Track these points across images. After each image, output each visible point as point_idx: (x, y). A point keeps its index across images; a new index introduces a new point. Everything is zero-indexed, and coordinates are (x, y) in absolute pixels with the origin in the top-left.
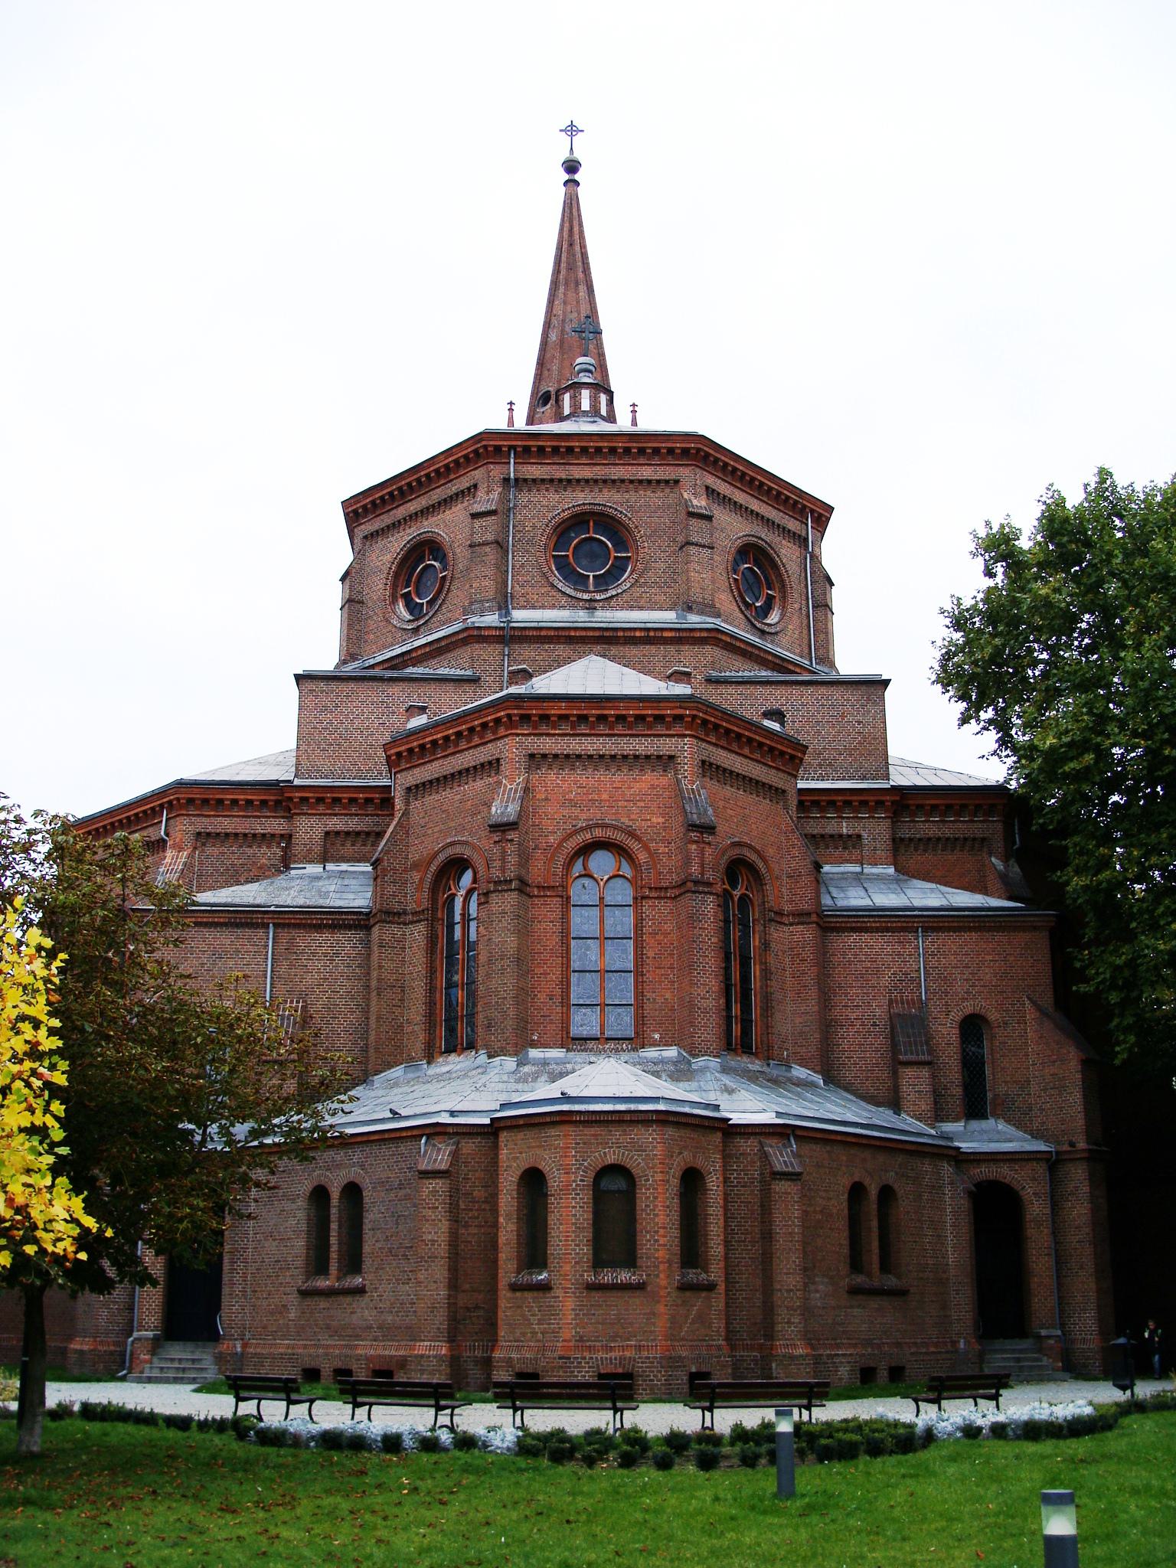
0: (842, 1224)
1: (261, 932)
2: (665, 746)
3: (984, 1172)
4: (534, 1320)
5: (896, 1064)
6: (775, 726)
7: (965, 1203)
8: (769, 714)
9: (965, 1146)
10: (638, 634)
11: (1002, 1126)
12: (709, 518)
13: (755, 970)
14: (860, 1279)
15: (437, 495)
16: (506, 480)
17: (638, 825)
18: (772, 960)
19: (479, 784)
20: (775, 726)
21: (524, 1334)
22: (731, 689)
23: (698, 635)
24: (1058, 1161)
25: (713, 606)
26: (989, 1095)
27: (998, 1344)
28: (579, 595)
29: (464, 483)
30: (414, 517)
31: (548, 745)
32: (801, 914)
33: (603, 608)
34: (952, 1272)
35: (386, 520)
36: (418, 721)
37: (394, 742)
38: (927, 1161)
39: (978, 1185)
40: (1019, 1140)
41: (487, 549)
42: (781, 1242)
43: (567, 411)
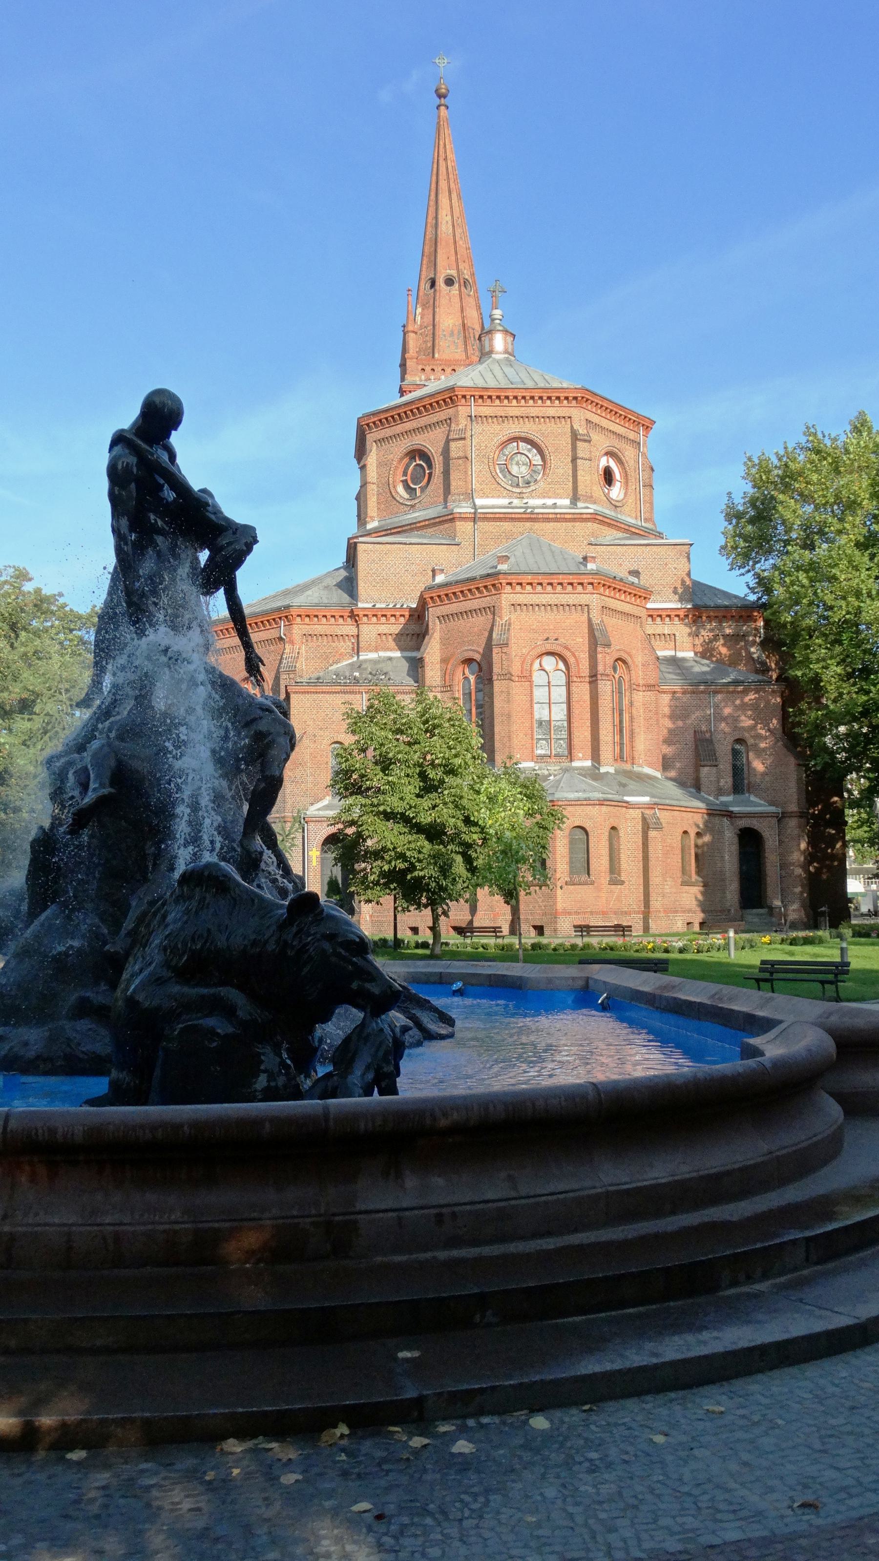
0: (678, 852)
1: (358, 696)
2: (584, 599)
3: (743, 823)
4: (540, 900)
5: (698, 767)
6: (636, 580)
7: (736, 840)
8: (630, 573)
9: (735, 809)
10: (551, 516)
11: (753, 798)
12: (590, 441)
13: (626, 717)
16: (471, 416)
17: (570, 643)
18: (634, 712)
20: (636, 580)
21: (534, 907)
23: (585, 516)
24: (783, 817)
25: (592, 497)
26: (746, 781)
27: (749, 911)
28: (514, 490)
31: (521, 599)
33: (528, 497)
34: (728, 874)
35: (388, 432)
36: (440, 579)
37: (430, 588)
38: (717, 818)
39: (740, 830)
41: (460, 461)
43: (487, 349)
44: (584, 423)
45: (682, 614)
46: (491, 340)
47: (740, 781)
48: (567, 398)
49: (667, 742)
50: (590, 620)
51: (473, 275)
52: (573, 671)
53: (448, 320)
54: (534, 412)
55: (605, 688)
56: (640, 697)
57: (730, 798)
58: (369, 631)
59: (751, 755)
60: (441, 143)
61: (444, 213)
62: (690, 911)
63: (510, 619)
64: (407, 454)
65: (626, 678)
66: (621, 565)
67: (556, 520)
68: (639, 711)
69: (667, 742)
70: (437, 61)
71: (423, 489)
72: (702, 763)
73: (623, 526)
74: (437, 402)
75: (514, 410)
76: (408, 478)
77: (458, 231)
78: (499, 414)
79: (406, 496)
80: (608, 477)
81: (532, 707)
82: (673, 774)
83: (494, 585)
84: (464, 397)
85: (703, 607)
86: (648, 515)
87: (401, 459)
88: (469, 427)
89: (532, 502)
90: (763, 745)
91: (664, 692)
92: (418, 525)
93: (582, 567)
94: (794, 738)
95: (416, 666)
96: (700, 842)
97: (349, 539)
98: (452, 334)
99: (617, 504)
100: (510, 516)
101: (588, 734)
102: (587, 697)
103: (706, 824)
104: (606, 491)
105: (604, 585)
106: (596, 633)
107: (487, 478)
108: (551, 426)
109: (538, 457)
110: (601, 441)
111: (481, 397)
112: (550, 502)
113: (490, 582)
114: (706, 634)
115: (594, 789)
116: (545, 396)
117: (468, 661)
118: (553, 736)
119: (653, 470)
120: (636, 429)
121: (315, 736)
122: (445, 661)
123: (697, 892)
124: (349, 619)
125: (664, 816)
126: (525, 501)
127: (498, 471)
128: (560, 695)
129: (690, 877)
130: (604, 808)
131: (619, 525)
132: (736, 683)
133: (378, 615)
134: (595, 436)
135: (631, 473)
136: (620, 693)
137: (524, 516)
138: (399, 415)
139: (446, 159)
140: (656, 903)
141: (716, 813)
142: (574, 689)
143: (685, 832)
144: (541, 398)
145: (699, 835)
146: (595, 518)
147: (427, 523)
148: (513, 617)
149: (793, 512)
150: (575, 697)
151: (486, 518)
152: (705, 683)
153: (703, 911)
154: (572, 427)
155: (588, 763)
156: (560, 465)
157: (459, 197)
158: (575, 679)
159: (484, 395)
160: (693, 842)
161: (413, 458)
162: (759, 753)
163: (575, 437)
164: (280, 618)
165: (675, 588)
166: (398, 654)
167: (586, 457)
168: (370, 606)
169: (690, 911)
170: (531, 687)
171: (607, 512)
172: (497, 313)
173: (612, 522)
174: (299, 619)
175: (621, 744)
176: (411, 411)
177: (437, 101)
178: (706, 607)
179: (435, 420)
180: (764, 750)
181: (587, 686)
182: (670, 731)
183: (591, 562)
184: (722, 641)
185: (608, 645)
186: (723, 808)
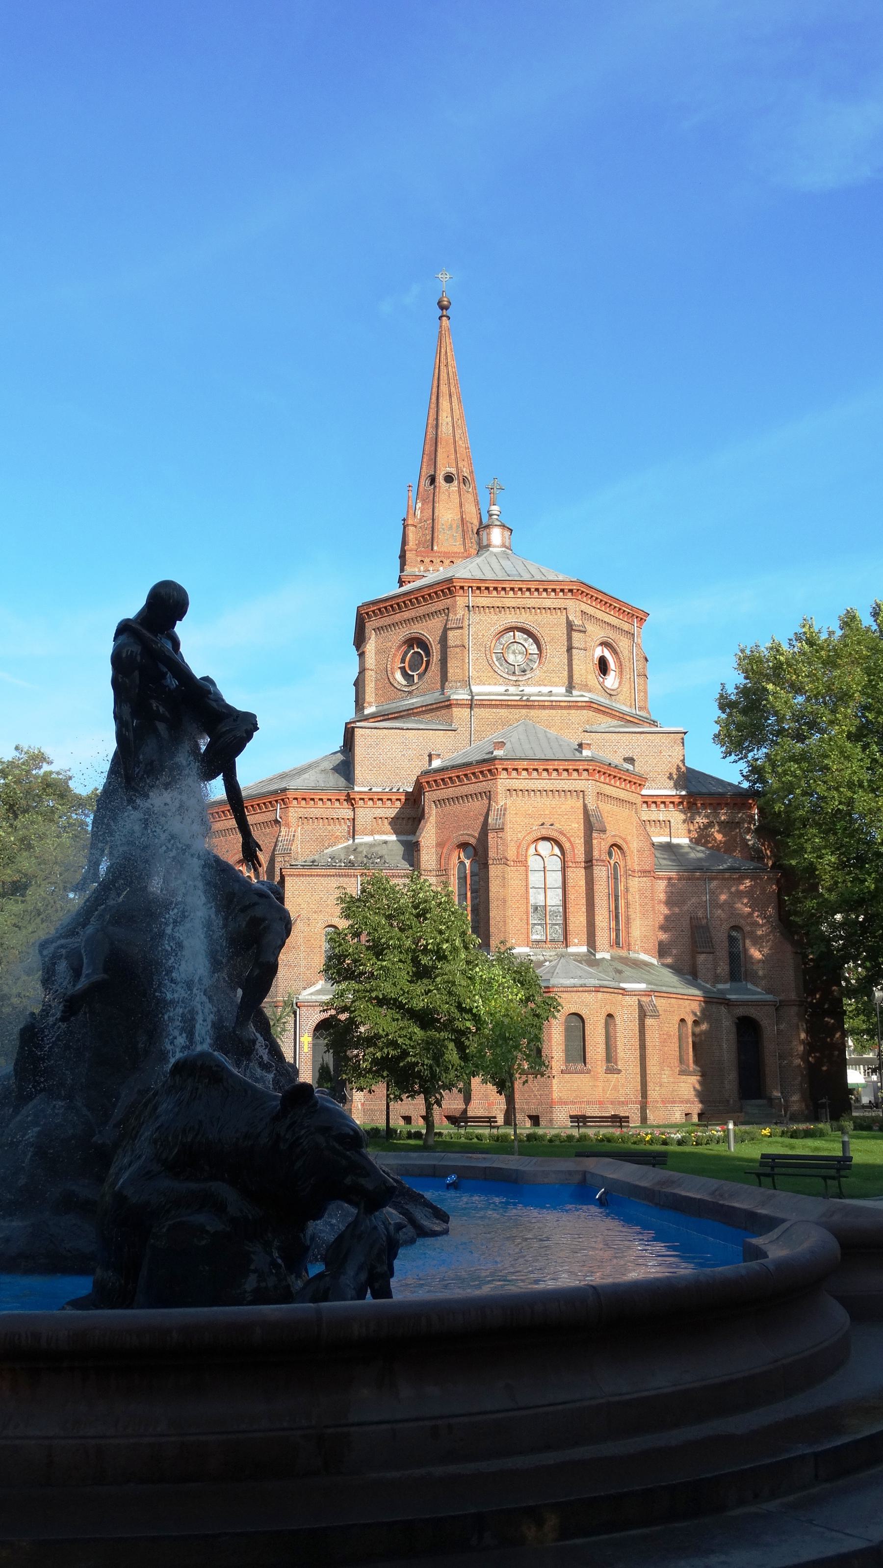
0: (676, 1040)
2: (580, 785)
3: (741, 1011)
6: (630, 767)
9: (733, 997)
10: (546, 704)
11: (750, 986)
13: (622, 903)
14: (684, 1067)
15: (422, 611)
16: (468, 607)
17: (566, 828)
19: (478, 805)
20: (630, 767)
21: (530, 1096)
22: (598, 735)
23: (580, 704)
25: (587, 685)
26: (743, 969)
28: (511, 677)
29: (440, 605)
30: (407, 621)
32: (645, 872)
33: (524, 685)
35: (386, 621)
36: (436, 763)
37: (426, 773)
39: (738, 1018)
40: (759, 993)
41: (458, 650)
42: (649, 1051)
43: (485, 543)
44: (579, 614)
45: (677, 800)
46: (488, 534)
47: (738, 966)
48: (562, 590)
49: (663, 928)
50: (585, 806)
51: (471, 472)
52: (569, 857)
53: (447, 514)
54: (531, 603)
55: (601, 873)
56: (635, 883)
57: (727, 986)
58: (365, 814)
59: (748, 942)
60: (443, 351)
61: (445, 415)
62: (687, 1101)
63: (505, 804)
64: (405, 642)
65: (622, 864)
66: (616, 752)
67: (552, 707)
68: (634, 897)
69: (663, 928)
70: (440, 276)
71: (420, 676)
72: (699, 950)
73: (617, 714)
74: (436, 593)
75: (510, 600)
76: (406, 665)
77: (458, 432)
78: (496, 605)
79: (404, 682)
80: (603, 666)
81: (527, 892)
82: (669, 960)
83: (490, 771)
84: (462, 588)
85: (697, 792)
86: (642, 703)
87: (400, 647)
88: (466, 617)
89: (528, 690)
90: (759, 933)
91: (660, 879)
92: (415, 711)
93: (577, 754)
94: (790, 926)
95: (411, 851)
96: (697, 1030)
97: (347, 724)
98: (451, 528)
99: (612, 693)
100: (506, 703)
101: (583, 919)
102: (583, 883)
103: (703, 1011)
104: (601, 680)
105: (599, 772)
106: (591, 819)
107: (483, 666)
108: (547, 617)
109: (535, 646)
110: (597, 633)
111: (479, 588)
112: (545, 690)
113: (486, 767)
114: (701, 820)
115: (592, 976)
116: (541, 587)
117: (463, 846)
118: (548, 921)
119: (647, 660)
120: (630, 621)
121: (309, 920)
122: (440, 845)
123: (695, 1081)
124: (345, 803)
125: (660, 1003)
126: (521, 689)
127: (495, 659)
128: (556, 881)
129: (688, 1066)
130: (600, 995)
131: (614, 713)
132: (731, 869)
133: (373, 798)
134: (590, 627)
135: (626, 663)
136: (616, 878)
137: (520, 703)
138: (398, 604)
139: (447, 365)
140: (654, 1093)
141: (711, 1001)
142: (570, 873)
143: (682, 1020)
144: (537, 590)
145: (696, 1023)
146: (590, 706)
147: (424, 709)
148: (509, 802)
149: (786, 702)
150: (570, 883)
151: (483, 705)
152: (700, 869)
153: (701, 1102)
154: (567, 617)
155: (584, 949)
156: (556, 653)
157: (459, 399)
158: (570, 864)
159: (481, 587)
160: (690, 1031)
161: (411, 646)
162: (757, 941)
163: (570, 627)
164: (276, 801)
165: (671, 774)
166: (394, 838)
167: (582, 646)
168: (366, 789)
169: (687, 1101)
170: (527, 871)
171: (602, 700)
172: (495, 509)
173: (607, 710)
174: (295, 802)
175: (617, 930)
176: (410, 600)
177: (439, 312)
178: (700, 794)
179: (433, 609)
180: (761, 937)
181: (583, 871)
182: (667, 918)
183: (586, 748)
184: (717, 828)
185: (604, 831)
186: (721, 996)
